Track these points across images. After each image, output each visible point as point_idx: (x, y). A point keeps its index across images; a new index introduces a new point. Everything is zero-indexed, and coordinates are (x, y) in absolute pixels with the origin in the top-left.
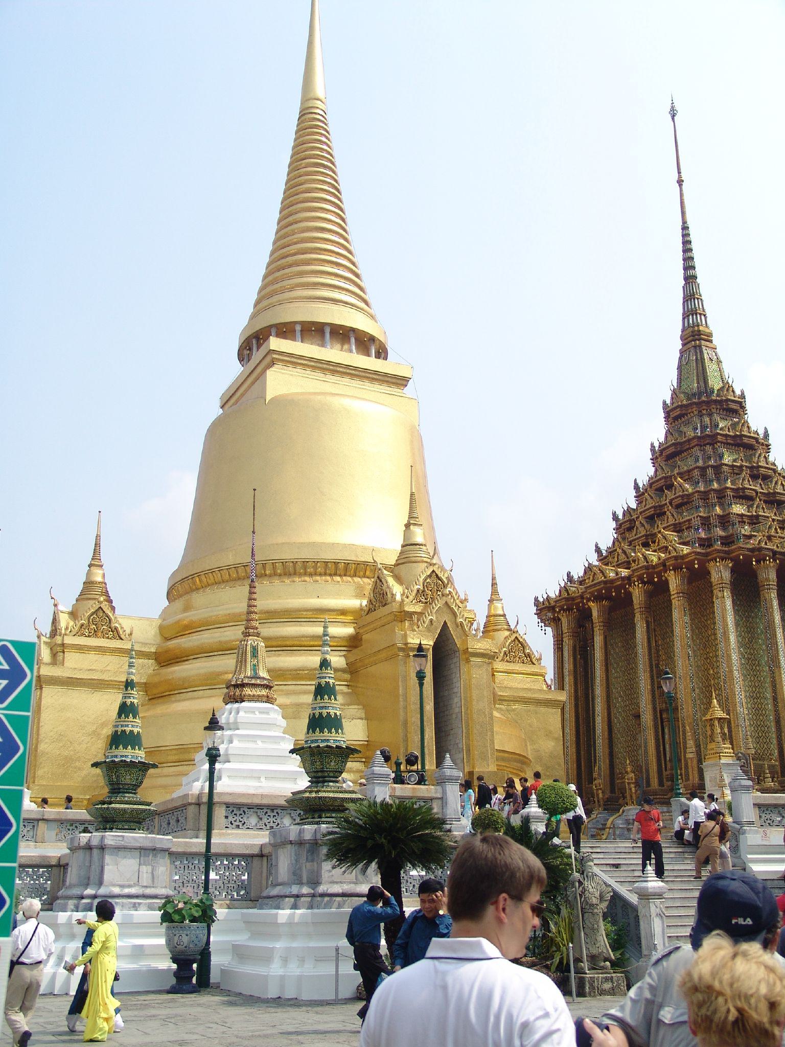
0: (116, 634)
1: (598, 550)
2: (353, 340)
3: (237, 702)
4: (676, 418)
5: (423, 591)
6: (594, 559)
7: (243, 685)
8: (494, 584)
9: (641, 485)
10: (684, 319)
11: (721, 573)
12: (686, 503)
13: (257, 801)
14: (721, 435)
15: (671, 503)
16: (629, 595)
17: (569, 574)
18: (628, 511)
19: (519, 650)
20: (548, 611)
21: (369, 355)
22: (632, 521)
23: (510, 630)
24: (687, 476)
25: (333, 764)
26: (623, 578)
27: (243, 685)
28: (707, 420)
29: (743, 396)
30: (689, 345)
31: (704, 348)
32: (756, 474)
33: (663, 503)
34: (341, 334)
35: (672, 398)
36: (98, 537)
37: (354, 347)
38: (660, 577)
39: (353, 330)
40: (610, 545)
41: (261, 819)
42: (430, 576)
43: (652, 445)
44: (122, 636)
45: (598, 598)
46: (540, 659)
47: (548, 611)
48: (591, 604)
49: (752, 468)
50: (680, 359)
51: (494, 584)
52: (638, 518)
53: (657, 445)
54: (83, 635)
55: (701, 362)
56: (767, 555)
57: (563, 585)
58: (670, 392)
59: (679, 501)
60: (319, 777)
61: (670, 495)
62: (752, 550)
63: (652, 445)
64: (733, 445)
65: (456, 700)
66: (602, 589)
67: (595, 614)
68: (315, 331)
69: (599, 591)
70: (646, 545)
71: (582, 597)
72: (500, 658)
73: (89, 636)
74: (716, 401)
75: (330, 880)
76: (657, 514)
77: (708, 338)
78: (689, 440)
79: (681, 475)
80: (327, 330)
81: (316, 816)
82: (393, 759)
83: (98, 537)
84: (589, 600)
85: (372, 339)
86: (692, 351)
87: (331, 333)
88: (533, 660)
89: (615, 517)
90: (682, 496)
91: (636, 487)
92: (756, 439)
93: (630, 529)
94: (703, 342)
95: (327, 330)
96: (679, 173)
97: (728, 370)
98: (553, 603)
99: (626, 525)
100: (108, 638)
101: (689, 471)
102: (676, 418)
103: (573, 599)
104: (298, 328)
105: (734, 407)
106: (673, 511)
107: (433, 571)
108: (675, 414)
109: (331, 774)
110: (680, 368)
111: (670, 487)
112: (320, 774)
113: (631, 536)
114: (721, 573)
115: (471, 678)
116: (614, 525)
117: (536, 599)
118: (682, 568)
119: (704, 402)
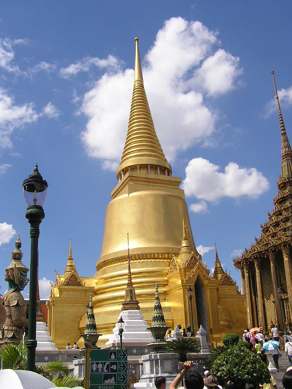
0: (79, 284)
1: (256, 240)
2: (159, 169)
3: (127, 310)
4: (282, 187)
5: (190, 264)
6: (254, 243)
7: (128, 304)
8: (217, 256)
13: (136, 345)
16: (268, 256)
17: (246, 249)
19: (228, 281)
20: (238, 264)
21: (164, 174)
22: (268, 228)
23: (224, 273)
25: (162, 332)
26: (265, 250)
27: (128, 304)
33: (279, 220)
34: (154, 167)
37: (159, 172)
39: (159, 166)
41: (138, 351)
42: (192, 258)
44: (82, 285)
45: (256, 258)
46: (236, 283)
48: (254, 260)
51: (217, 256)
52: (270, 226)
54: (68, 285)
60: (157, 337)
61: (281, 217)
65: (204, 303)
66: (257, 255)
68: (144, 167)
69: (257, 255)
70: (273, 237)
71: (250, 258)
73: (70, 285)
75: (164, 372)
76: (277, 224)
80: (149, 167)
81: (157, 350)
82: (182, 328)
85: (166, 168)
86: (286, 161)
87: (151, 167)
88: (233, 284)
93: (267, 231)
95: (149, 167)
100: (76, 285)
101: (288, 208)
104: (138, 166)
106: (282, 224)
107: (193, 256)
109: (162, 336)
111: (281, 214)
112: (158, 336)
113: (268, 234)
115: (208, 295)
118: (287, 246)
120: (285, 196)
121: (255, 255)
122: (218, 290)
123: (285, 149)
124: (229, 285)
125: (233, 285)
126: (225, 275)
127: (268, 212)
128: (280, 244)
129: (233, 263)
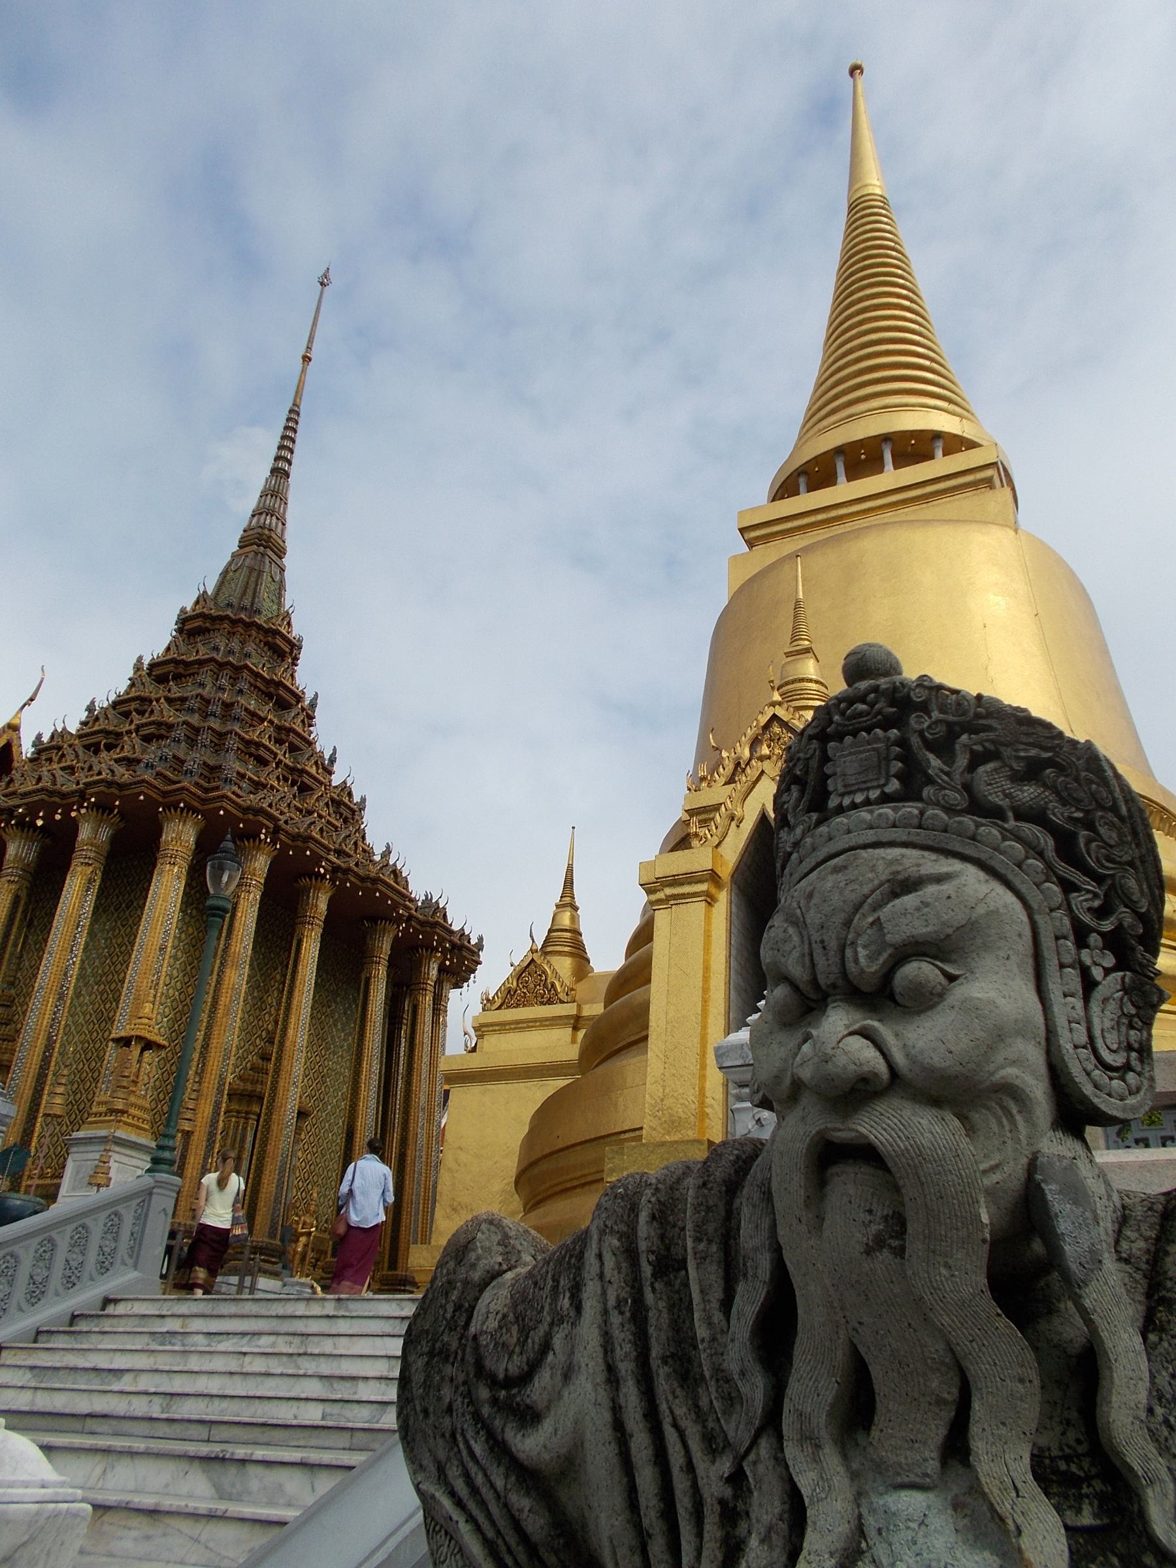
10: (253, 516)
11: (180, 837)
12: (161, 737)
14: (250, 670)
15: (137, 730)
18: (60, 736)
24: (177, 702)
28: (235, 645)
29: (300, 640)
31: (267, 560)
32: (282, 734)
35: (197, 602)
38: (66, 814)
43: (140, 659)
49: (279, 728)
50: (230, 564)
53: (146, 661)
55: (256, 573)
56: (263, 825)
59: (152, 730)
62: (246, 810)
63: (140, 659)
64: (263, 692)
74: (259, 627)
77: (281, 552)
78: (201, 663)
79: (169, 701)
86: (251, 555)
90: (159, 724)
92: (299, 698)
94: (270, 553)
96: (309, 348)
97: (290, 598)
101: (183, 700)
105: (285, 649)
108: (191, 626)
110: (225, 573)
114: (180, 837)
119: (241, 620)
120: (192, 659)
123: (264, 516)
128: (82, 795)
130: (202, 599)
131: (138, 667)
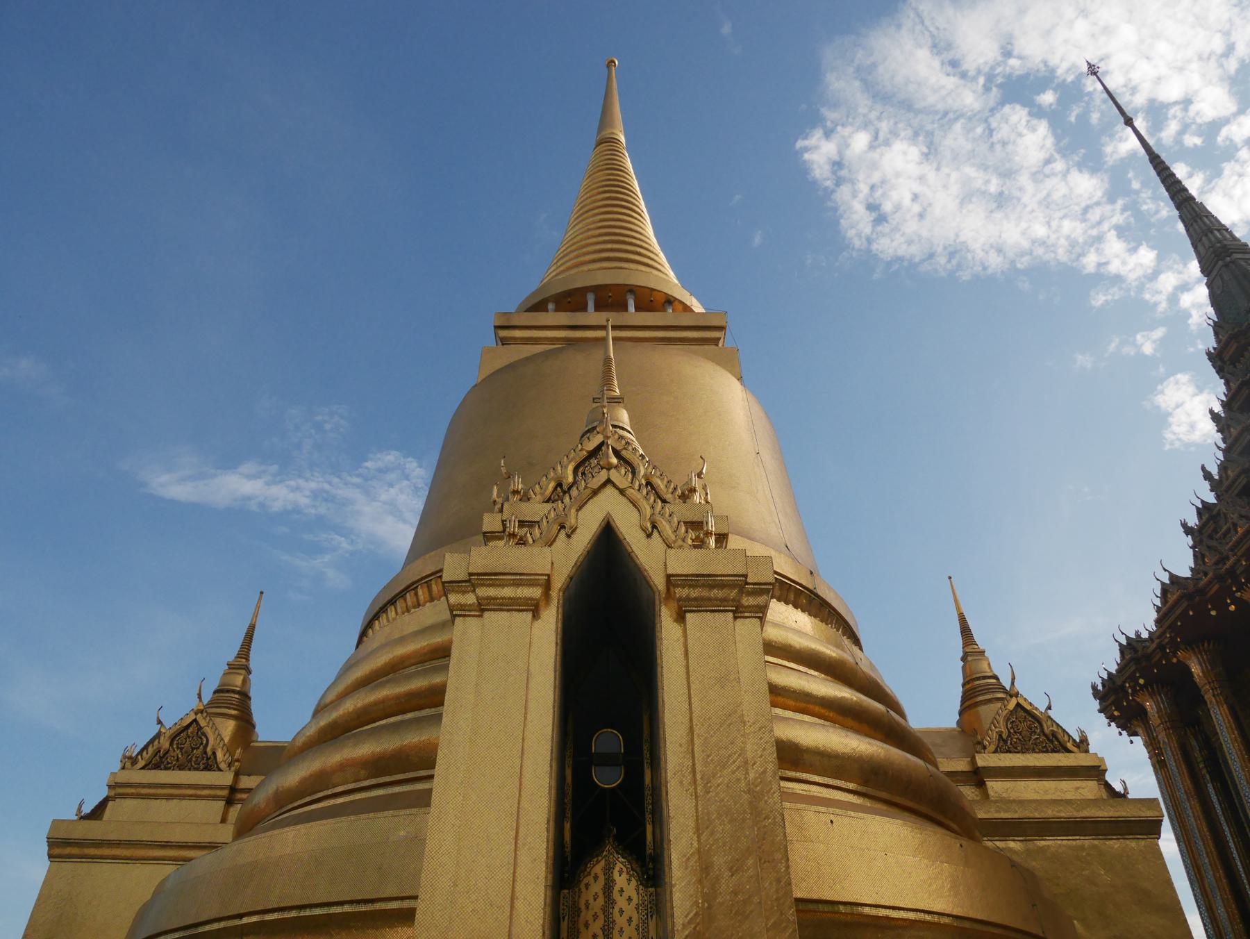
4: (1234, 361)
8: (966, 631)
9: (1214, 471)
18: (1204, 509)
19: (1033, 730)
20: (1117, 700)
30: (1214, 273)
36: (252, 629)
37: (631, 308)
39: (632, 289)
40: (1191, 563)
44: (223, 766)
47: (1117, 700)
51: (966, 631)
53: (1218, 408)
54: (157, 767)
57: (1124, 642)
58: (1211, 330)
66: (1185, 612)
67: (1196, 669)
71: (1161, 647)
72: (992, 748)
83: (252, 629)
84: (1175, 648)
88: (1069, 745)
89: (1188, 530)
91: (1207, 476)
98: (1119, 682)
99: (1207, 531)
100: (197, 769)
102: (1234, 361)
103: (1148, 657)
116: (1189, 540)
117: (1094, 687)
121: (1174, 616)
122: (981, 784)
124: (1047, 752)
125: (1068, 751)
126: (1013, 702)
127: (1203, 468)
129: (1096, 704)
130: (1217, 328)
131: (1215, 416)
